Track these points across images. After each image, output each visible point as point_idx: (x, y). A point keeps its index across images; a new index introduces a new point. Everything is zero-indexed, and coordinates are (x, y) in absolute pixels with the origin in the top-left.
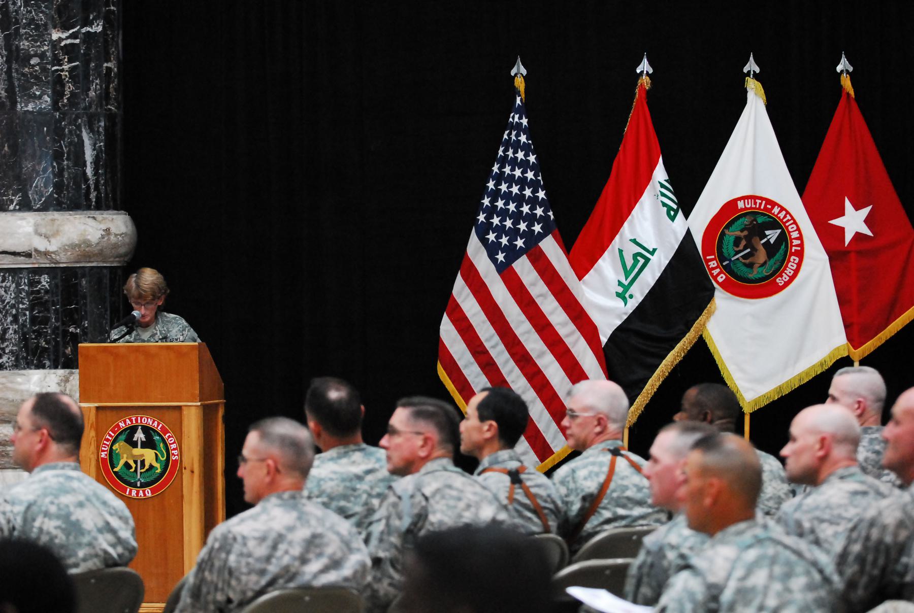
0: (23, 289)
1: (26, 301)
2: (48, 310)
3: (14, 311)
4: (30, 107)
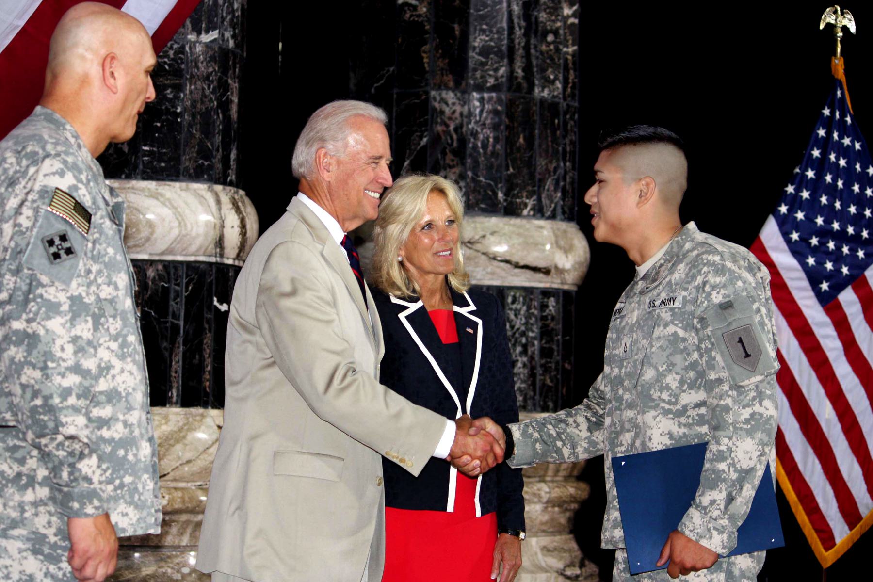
0: (533, 314)
1: (535, 328)
3: (524, 340)
4: (546, 93)
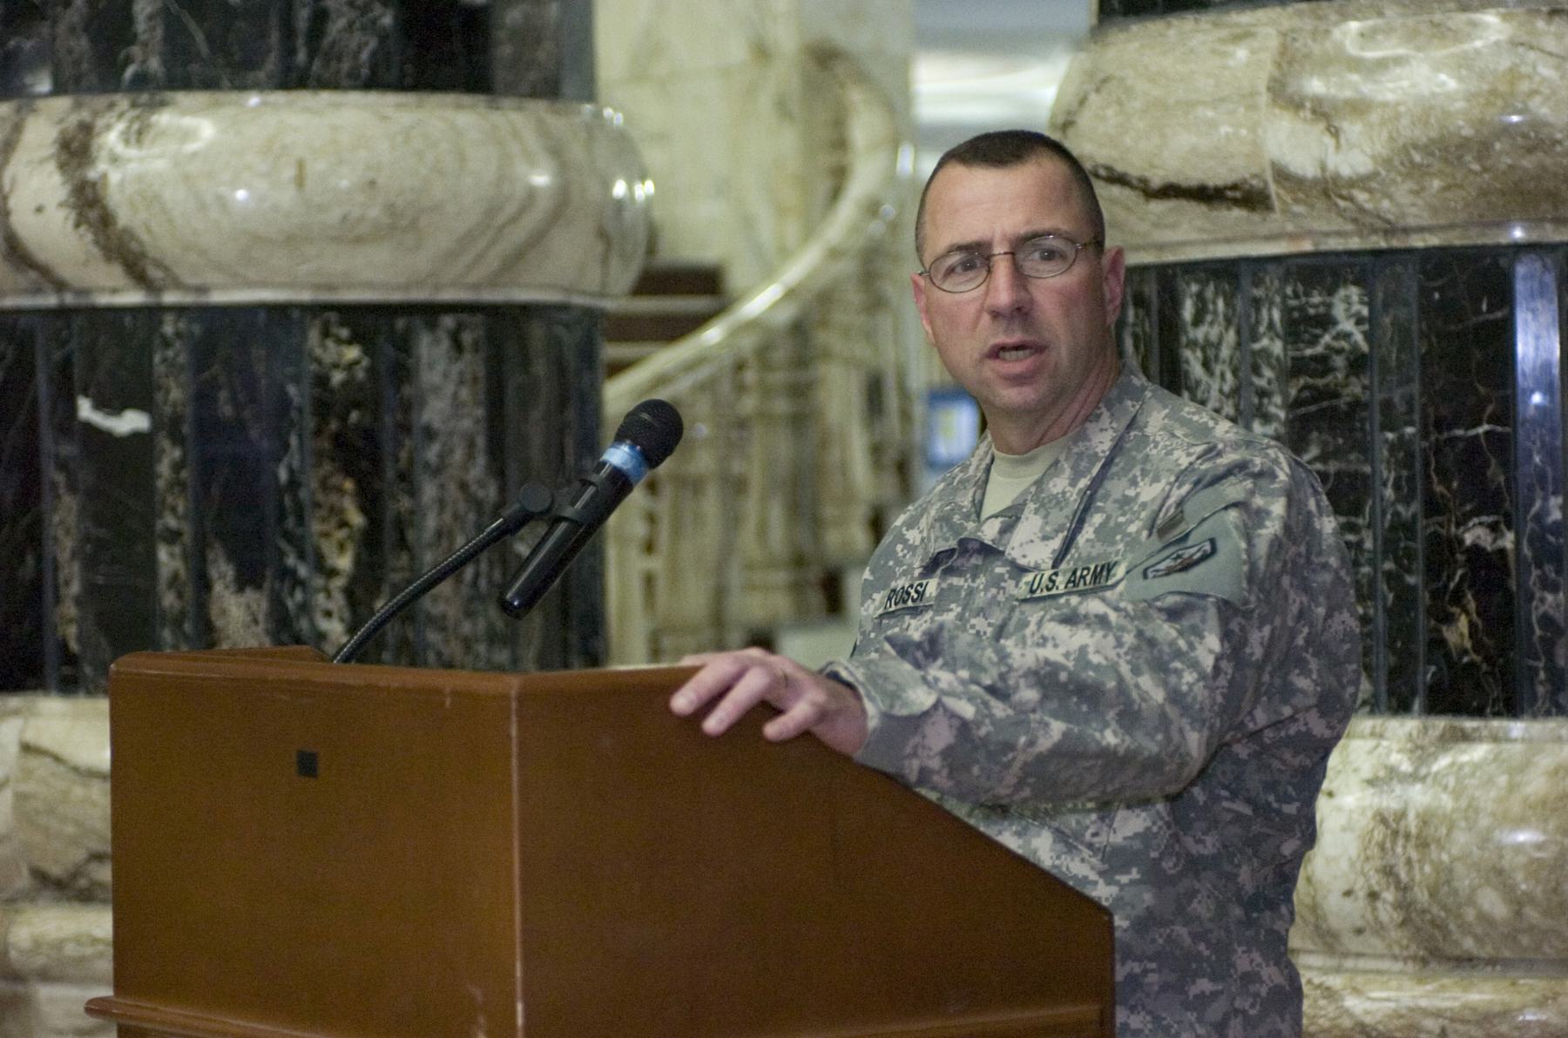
0: (1265, 353)
2: (1366, 450)
